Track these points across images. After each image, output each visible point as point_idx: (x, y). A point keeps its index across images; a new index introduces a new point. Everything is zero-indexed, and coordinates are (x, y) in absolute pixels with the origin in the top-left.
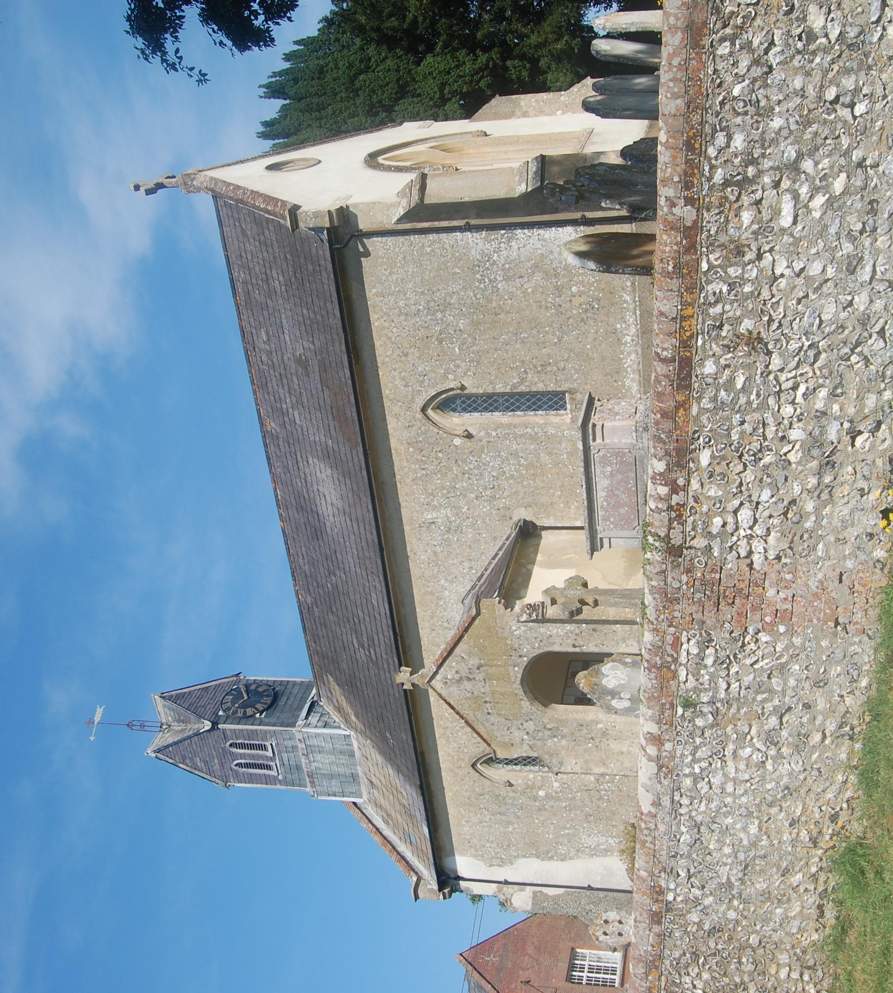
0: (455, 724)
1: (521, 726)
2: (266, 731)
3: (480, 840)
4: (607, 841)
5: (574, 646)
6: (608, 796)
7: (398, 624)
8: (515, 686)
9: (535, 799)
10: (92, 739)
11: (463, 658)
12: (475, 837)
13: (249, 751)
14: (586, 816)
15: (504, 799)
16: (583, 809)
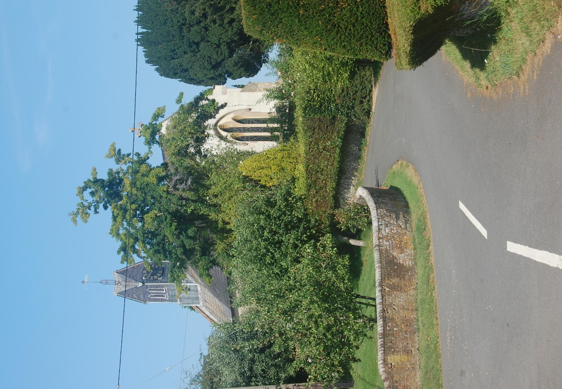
2: (165, 285)
10: (85, 289)
13: (156, 291)
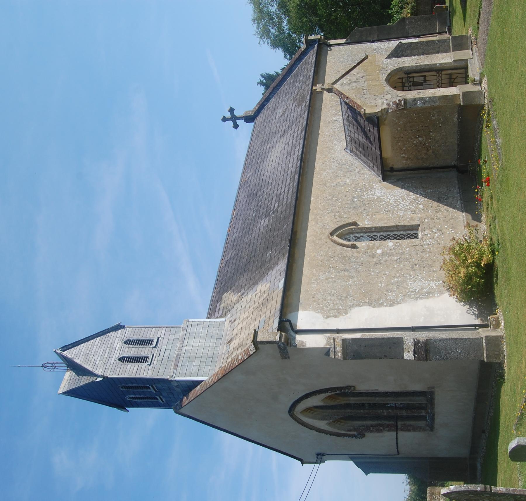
0: (325, 211)
1: (383, 97)
3: (323, 295)
4: (429, 285)
5: (416, 63)
6: (430, 249)
7: (303, 169)
8: (382, 81)
9: (373, 256)
11: (354, 74)
12: (320, 292)
14: (412, 265)
15: (349, 259)
16: (410, 260)
